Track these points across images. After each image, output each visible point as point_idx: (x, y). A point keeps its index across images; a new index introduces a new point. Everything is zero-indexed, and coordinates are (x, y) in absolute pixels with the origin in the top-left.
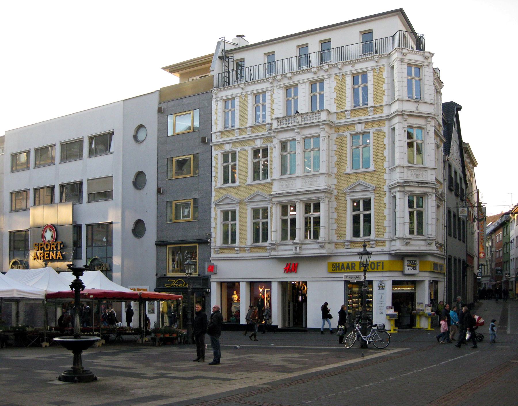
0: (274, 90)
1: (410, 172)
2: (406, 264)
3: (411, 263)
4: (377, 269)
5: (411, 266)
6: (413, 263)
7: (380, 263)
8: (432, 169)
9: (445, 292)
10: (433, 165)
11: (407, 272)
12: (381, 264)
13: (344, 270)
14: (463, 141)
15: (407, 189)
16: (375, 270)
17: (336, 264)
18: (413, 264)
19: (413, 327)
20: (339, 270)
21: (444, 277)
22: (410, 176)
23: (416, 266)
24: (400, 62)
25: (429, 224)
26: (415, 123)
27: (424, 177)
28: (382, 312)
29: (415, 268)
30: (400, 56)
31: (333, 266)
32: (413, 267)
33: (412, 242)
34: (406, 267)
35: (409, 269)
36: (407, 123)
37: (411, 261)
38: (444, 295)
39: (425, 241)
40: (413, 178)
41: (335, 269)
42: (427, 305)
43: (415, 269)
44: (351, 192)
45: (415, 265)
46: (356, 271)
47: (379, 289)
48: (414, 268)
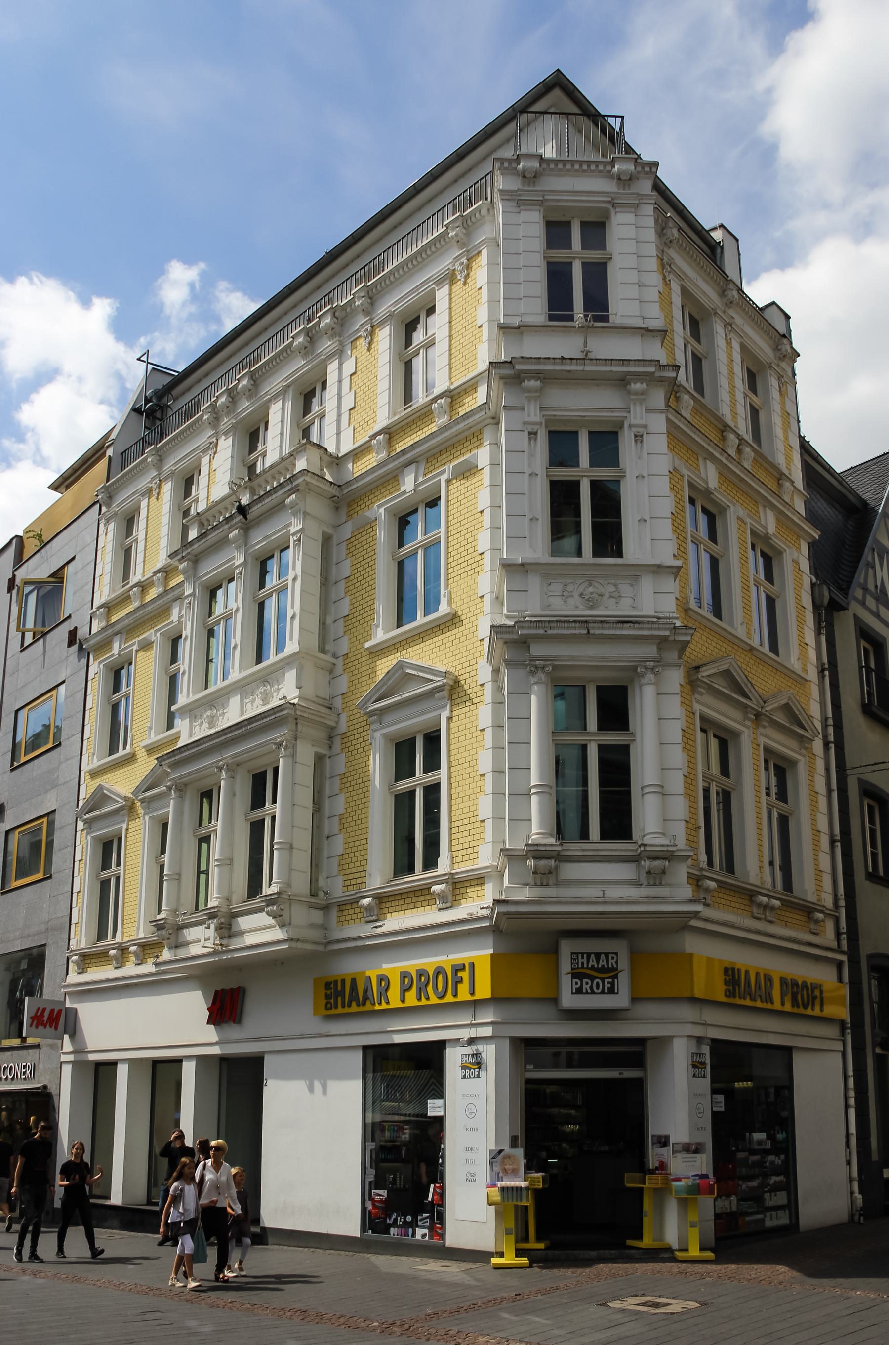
0: (217, 444)
1: (557, 588)
2: (566, 966)
3: (593, 962)
4: (455, 995)
5: (592, 978)
6: (603, 962)
7: (462, 968)
8: (658, 569)
9: (852, 1093)
10: (666, 555)
11: (568, 1000)
12: (465, 975)
13: (358, 1005)
14: (838, 471)
15: (537, 650)
16: (449, 998)
17: (336, 982)
18: (603, 970)
19: (630, 1242)
20: (343, 1006)
21: (843, 1034)
22: (557, 602)
23: (616, 977)
24: (514, 204)
25: (646, 790)
26: (585, 404)
27: (626, 602)
28: (473, 1175)
29: (612, 984)
30: (514, 184)
31: (329, 992)
32: (603, 979)
33: (570, 871)
34: (566, 984)
35: (579, 991)
36: (541, 409)
37: (589, 955)
38: (847, 1107)
39: (633, 866)
40: (575, 608)
41: (332, 1001)
42: (679, 1148)
43: (612, 991)
44: (382, 711)
45: (612, 973)
46: (391, 1006)
47: (464, 1077)
48: (607, 986)
